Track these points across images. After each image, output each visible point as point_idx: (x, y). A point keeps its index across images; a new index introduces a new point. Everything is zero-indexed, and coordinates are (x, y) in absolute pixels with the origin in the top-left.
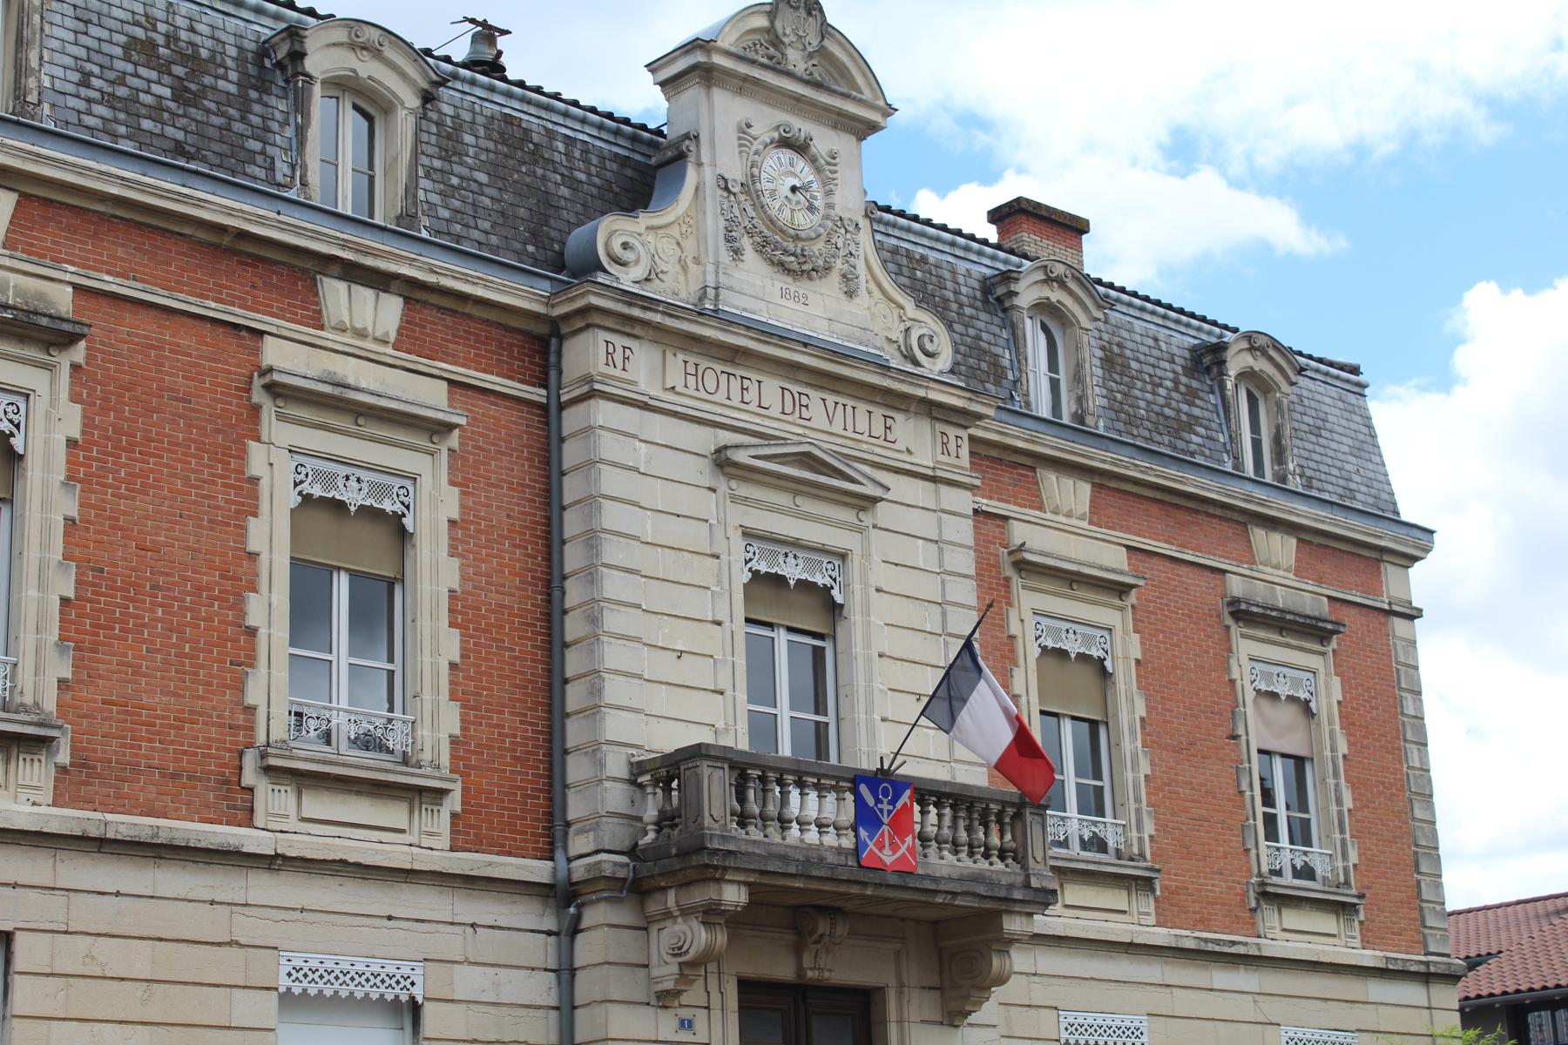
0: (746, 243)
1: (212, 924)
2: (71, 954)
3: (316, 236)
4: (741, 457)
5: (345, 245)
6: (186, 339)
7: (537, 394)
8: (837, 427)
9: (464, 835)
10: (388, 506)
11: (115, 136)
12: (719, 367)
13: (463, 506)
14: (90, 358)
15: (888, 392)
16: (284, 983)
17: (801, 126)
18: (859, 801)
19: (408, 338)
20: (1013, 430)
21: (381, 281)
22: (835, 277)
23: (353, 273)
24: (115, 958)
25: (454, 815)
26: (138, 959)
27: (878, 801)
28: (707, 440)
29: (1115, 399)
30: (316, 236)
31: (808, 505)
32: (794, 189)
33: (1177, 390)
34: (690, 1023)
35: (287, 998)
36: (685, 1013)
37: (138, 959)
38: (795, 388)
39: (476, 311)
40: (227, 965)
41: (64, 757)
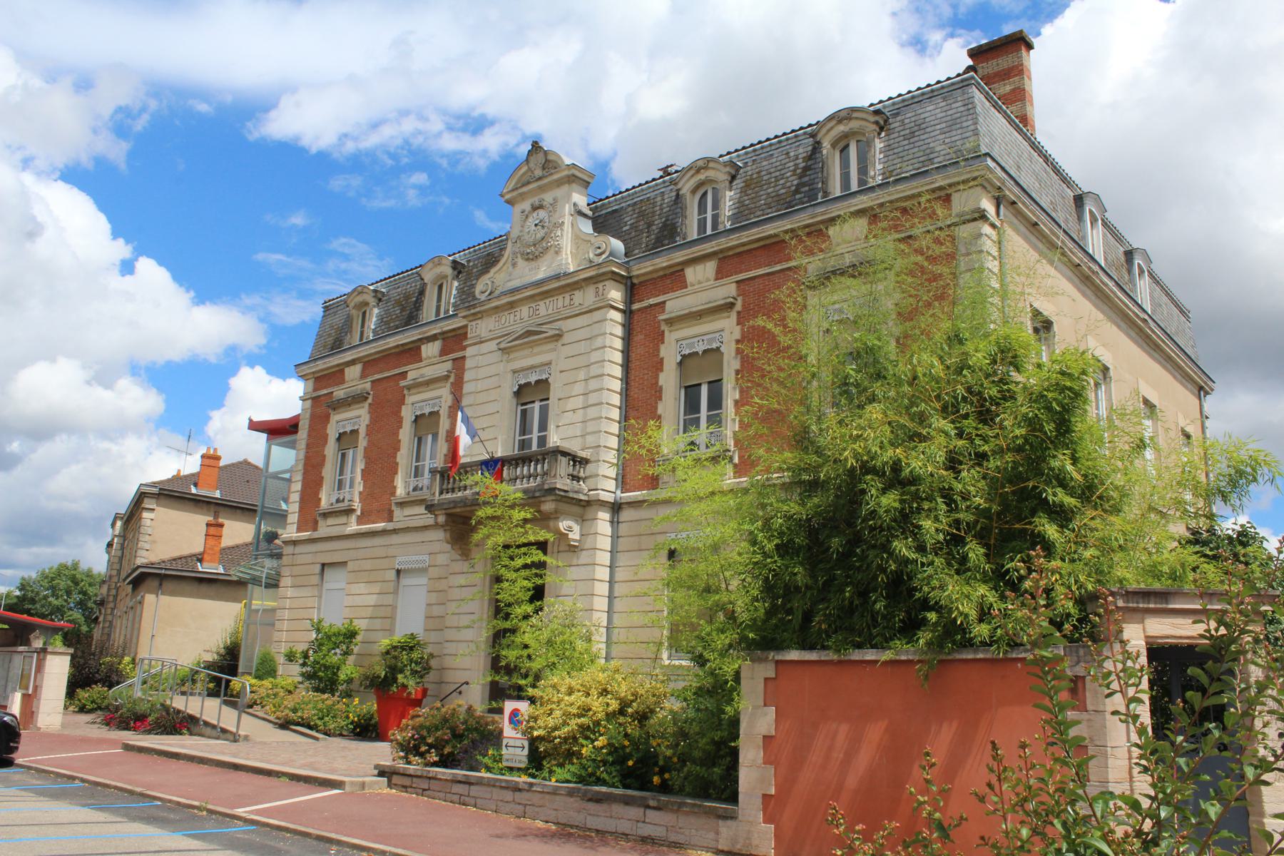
3: (413, 336)
4: (502, 346)
5: (420, 334)
8: (550, 311)
12: (506, 313)
15: (568, 285)
16: (397, 567)
17: (535, 200)
20: (658, 260)
26: (367, 565)
31: (536, 350)
32: (536, 225)
38: (533, 305)
39: (450, 335)
41: (359, 513)
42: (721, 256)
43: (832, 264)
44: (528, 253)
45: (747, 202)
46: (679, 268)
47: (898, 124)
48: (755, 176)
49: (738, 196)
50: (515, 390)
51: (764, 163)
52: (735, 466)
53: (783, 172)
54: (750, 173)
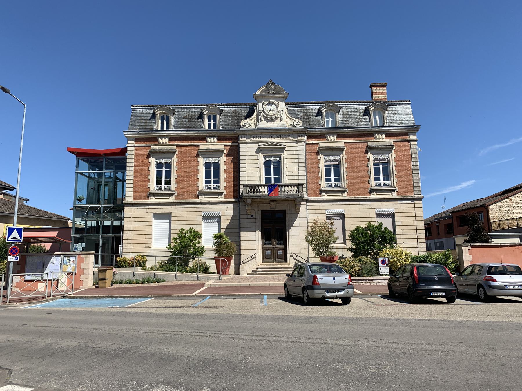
1: (194, 210)
2: (178, 214)
5: (207, 133)
6: (190, 148)
7: (237, 144)
9: (226, 197)
10: (217, 161)
11: (181, 128)
13: (226, 159)
14: (178, 153)
17: (271, 100)
18: (269, 188)
21: (214, 136)
22: (279, 119)
24: (182, 214)
25: (225, 195)
26: (186, 214)
27: (272, 188)
28: (257, 145)
29: (344, 120)
30: (203, 133)
33: (360, 115)
34: (253, 216)
35: (203, 216)
36: (253, 215)
37: (186, 214)
40: (196, 214)
41: (176, 194)
42: (338, 134)
43: (375, 143)
44: (269, 118)
45: (345, 120)
46: (324, 134)
47: (391, 110)
48: (346, 112)
49: (342, 117)
50: (264, 161)
51: (349, 109)
52: (347, 193)
53: (356, 114)
54: (344, 111)
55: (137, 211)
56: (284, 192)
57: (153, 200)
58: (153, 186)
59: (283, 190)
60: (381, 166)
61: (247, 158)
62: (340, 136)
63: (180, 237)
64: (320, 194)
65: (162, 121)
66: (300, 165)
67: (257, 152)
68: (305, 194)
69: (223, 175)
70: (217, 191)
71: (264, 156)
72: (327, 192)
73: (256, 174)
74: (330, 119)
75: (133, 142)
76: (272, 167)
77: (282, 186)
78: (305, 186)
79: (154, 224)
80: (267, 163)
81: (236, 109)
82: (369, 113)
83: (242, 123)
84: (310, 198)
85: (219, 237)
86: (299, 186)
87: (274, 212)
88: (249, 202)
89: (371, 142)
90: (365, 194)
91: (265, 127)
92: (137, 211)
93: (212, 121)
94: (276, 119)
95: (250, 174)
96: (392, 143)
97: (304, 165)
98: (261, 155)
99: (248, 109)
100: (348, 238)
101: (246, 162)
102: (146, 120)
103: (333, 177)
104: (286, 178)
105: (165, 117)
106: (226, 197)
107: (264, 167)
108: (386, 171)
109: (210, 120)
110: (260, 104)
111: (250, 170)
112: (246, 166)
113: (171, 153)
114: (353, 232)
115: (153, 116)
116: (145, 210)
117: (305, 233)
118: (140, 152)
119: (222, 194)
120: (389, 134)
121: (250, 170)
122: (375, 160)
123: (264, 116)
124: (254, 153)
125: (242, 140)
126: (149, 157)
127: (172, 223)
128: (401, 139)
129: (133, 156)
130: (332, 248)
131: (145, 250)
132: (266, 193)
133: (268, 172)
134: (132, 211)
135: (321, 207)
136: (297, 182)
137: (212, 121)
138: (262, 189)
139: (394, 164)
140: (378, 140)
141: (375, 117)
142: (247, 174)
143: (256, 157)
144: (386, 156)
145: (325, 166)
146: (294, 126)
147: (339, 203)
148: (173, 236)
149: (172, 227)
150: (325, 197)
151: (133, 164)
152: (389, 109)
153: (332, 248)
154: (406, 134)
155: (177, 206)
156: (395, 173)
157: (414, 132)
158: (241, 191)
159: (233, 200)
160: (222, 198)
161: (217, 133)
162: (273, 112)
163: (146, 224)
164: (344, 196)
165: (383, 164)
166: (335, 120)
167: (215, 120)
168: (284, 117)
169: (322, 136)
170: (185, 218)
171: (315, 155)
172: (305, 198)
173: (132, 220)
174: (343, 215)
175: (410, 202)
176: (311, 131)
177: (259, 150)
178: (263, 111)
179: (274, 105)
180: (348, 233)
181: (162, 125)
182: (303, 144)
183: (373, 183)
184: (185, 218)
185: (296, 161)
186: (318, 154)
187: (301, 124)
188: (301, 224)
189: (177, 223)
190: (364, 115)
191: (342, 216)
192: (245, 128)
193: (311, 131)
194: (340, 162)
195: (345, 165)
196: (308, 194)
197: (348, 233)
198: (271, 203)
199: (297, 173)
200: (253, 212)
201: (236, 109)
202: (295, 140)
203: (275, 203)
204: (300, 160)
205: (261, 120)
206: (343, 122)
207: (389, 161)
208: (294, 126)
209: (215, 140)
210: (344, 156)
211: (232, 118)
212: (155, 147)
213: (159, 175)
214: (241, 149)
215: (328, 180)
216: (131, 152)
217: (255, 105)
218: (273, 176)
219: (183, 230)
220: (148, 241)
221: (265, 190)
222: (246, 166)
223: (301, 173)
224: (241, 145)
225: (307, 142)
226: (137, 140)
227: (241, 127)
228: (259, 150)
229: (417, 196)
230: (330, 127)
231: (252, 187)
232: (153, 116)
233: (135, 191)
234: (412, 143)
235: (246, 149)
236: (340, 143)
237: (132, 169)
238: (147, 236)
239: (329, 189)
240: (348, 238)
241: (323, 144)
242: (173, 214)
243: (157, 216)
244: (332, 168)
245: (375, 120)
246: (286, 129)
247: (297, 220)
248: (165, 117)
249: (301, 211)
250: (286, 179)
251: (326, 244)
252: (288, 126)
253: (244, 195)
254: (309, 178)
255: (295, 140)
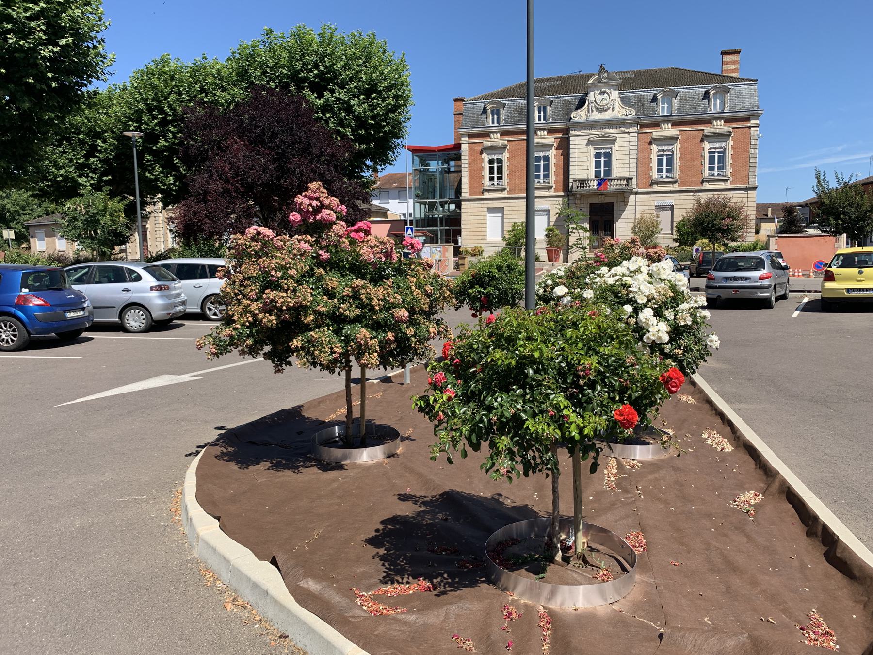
0: (594, 109)
2: (510, 208)
6: (520, 142)
9: (555, 190)
17: (604, 90)
19: (548, 133)
21: (544, 129)
23: (540, 129)
24: (514, 208)
26: (517, 208)
28: (587, 138)
37: (517, 208)
55: (473, 206)
56: (612, 187)
57: (487, 195)
58: (486, 182)
59: (612, 183)
60: (716, 155)
61: (577, 151)
62: (675, 124)
63: (513, 230)
64: (650, 185)
65: (493, 115)
66: (631, 156)
67: (587, 144)
68: (634, 186)
69: (552, 169)
70: (547, 185)
71: (595, 149)
72: (657, 183)
73: (586, 168)
74: (666, 105)
75: (467, 139)
76: (603, 159)
77: (612, 180)
78: (635, 178)
79: (488, 219)
80: (597, 156)
81: (567, 98)
82: (709, 97)
83: (573, 115)
84: (640, 190)
85: (550, 230)
86: (628, 179)
87: (602, 205)
88: (578, 196)
89: (708, 129)
90: (697, 185)
91: (596, 118)
92: (473, 206)
93: (542, 112)
94: (609, 109)
95: (580, 168)
96: (731, 130)
97: (635, 156)
98: (592, 147)
99: (579, 98)
100: (675, 229)
101: (576, 155)
102: (478, 115)
103: (665, 168)
104: (616, 170)
105: (495, 111)
106: (555, 190)
107: (594, 159)
108: (722, 160)
109: (540, 112)
110: (592, 93)
111: (580, 164)
112: (576, 159)
113: (502, 148)
114: (679, 223)
115: (485, 111)
116: (480, 206)
117: (632, 225)
118: (475, 148)
119: (551, 188)
120: (728, 120)
121: (580, 164)
122: (711, 148)
123: (595, 107)
124: (584, 146)
125: (572, 133)
126: (481, 153)
127: (505, 217)
128: (741, 125)
129: (467, 153)
130: (656, 238)
131: (482, 241)
132: (595, 187)
133: (598, 165)
134: (469, 206)
135: (651, 199)
136: (626, 175)
137: (542, 112)
138: (591, 183)
139: (730, 152)
140: (715, 127)
141: (715, 100)
142: (576, 168)
143: (586, 150)
144: (723, 144)
145: (658, 156)
146: (627, 116)
147: (669, 194)
148: (505, 229)
149: (505, 221)
150: (655, 188)
151: (467, 161)
152: (732, 91)
153: (656, 238)
154: (748, 119)
155: (509, 201)
156: (731, 161)
157: (757, 117)
158: (571, 185)
159: (562, 193)
160: (551, 192)
161: (547, 126)
162: (605, 102)
163: (482, 217)
164: (675, 187)
165: (719, 152)
166: (670, 106)
167: (545, 112)
168: (617, 106)
169: (656, 125)
170: (516, 212)
171: (647, 145)
172: (635, 190)
173: (469, 214)
174: (673, 206)
175: (743, 192)
176: (644, 120)
177: (590, 142)
178: (595, 101)
179: (606, 94)
180: (675, 224)
181: (493, 119)
182: (636, 134)
183: (707, 173)
184: (516, 212)
185: (627, 153)
186: (650, 144)
187: (634, 113)
188: (629, 216)
189: (509, 217)
190: (703, 99)
191: (671, 208)
192: (576, 119)
193: (644, 120)
194: (673, 152)
195: (679, 155)
196: (637, 185)
197: (675, 224)
198: (600, 196)
199: (627, 165)
200: (582, 205)
201: (567, 98)
202: (627, 130)
203: (604, 196)
204: (632, 152)
205: (592, 111)
206: (679, 109)
207: (725, 149)
208: (627, 116)
209: (546, 133)
210: (678, 145)
211: (563, 108)
212: (487, 143)
213: (491, 170)
214: (571, 142)
215: (660, 171)
216: (465, 148)
217: (587, 94)
218: (602, 169)
219: (515, 223)
220: (483, 233)
221: (594, 185)
222: (576, 159)
223: (631, 165)
224: (571, 138)
225: (640, 132)
226: (471, 136)
227: (571, 119)
228: (590, 142)
229: (751, 186)
230: (666, 114)
231: (582, 182)
232: (485, 111)
233: (470, 188)
234: (752, 129)
235: (577, 142)
236: (675, 132)
237: (467, 165)
238: (483, 229)
239: (661, 180)
240: (675, 229)
241: (657, 133)
242: (505, 209)
243: (491, 210)
244: (665, 158)
245: (715, 104)
246: (618, 120)
247: (625, 212)
248: (495, 111)
249: (629, 203)
250: (616, 172)
251: (651, 235)
252: (620, 116)
253: (574, 190)
254: (640, 169)
255: (627, 130)
